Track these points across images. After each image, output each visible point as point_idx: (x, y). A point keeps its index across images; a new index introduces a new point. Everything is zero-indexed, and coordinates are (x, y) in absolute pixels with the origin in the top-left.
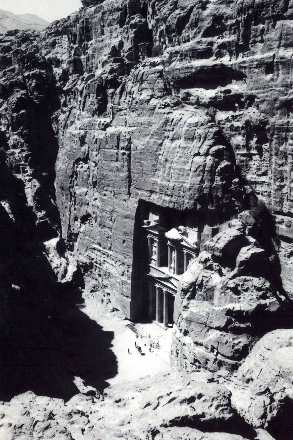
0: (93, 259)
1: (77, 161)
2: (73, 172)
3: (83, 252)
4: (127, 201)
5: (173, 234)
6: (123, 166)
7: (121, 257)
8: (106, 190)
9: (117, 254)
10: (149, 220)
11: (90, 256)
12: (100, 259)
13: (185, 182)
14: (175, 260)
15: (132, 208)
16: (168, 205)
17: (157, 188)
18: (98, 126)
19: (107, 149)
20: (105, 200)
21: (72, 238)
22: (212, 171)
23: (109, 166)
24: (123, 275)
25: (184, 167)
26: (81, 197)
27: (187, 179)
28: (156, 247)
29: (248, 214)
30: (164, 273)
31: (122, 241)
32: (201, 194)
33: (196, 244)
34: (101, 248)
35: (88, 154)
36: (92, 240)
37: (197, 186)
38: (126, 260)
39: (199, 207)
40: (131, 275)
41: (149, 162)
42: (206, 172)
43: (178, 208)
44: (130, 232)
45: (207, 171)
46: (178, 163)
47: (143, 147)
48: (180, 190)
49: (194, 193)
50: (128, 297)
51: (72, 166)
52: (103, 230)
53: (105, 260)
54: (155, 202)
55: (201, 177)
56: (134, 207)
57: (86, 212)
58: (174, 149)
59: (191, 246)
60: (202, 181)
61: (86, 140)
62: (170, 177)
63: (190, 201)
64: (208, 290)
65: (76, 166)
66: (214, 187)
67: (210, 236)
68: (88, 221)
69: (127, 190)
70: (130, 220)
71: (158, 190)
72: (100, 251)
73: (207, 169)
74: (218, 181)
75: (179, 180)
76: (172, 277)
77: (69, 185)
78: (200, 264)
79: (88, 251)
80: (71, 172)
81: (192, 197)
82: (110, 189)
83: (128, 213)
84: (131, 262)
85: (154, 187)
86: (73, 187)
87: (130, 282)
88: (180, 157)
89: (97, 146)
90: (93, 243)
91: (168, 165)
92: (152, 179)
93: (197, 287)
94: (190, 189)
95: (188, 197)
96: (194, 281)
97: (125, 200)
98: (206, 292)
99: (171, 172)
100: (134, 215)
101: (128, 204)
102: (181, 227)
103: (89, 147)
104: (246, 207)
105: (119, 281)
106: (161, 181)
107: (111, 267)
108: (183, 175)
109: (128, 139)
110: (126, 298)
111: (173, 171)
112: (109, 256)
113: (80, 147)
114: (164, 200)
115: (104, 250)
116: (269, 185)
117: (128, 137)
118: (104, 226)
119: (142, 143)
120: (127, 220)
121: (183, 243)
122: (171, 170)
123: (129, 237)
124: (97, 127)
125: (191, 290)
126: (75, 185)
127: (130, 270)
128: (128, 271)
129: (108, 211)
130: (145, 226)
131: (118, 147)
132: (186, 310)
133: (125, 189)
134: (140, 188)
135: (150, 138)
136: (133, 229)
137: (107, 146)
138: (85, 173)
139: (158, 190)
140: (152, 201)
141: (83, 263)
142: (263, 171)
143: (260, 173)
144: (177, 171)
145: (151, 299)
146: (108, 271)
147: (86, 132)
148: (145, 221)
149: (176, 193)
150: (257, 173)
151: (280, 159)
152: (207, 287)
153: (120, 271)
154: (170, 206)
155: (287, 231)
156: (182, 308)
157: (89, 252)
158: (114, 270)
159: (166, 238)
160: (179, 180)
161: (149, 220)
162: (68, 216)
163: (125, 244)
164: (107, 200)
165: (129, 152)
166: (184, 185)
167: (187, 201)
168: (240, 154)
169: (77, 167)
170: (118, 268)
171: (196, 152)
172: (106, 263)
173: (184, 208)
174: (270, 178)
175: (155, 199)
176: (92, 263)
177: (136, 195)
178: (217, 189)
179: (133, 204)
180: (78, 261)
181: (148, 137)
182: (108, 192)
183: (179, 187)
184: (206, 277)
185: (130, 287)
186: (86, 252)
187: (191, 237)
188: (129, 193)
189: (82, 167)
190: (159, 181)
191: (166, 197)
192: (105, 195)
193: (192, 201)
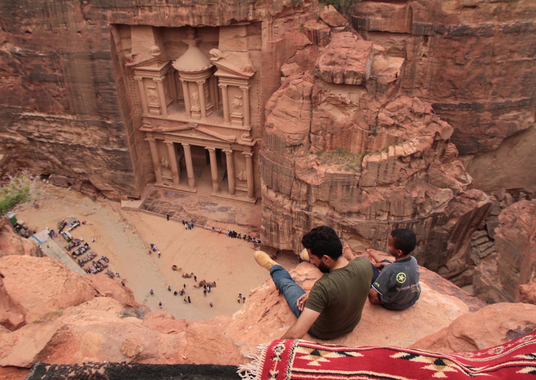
0: (31, 134)
20: (30, 40)
24: (106, 144)
29: (335, 10)
31: (94, 95)
33: (250, 70)
34: (42, 115)
53: (59, 129)
56: (104, 39)
59: (242, 75)
70: (102, 60)
72: (43, 119)
90: (24, 110)
93: (312, 136)
101: (89, 37)
105: (100, 152)
107: (75, 137)
112: (62, 124)
114: (177, 16)
115: (51, 116)
123: (107, 87)
125: (305, 141)
128: (117, 137)
130: (128, 64)
146: (70, 144)
153: (98, 138)
154: (191, 24)
155: (385, 24)
161: (133, 53)
167: (230, 9)
172: (62, 134)
182: (34, 26)
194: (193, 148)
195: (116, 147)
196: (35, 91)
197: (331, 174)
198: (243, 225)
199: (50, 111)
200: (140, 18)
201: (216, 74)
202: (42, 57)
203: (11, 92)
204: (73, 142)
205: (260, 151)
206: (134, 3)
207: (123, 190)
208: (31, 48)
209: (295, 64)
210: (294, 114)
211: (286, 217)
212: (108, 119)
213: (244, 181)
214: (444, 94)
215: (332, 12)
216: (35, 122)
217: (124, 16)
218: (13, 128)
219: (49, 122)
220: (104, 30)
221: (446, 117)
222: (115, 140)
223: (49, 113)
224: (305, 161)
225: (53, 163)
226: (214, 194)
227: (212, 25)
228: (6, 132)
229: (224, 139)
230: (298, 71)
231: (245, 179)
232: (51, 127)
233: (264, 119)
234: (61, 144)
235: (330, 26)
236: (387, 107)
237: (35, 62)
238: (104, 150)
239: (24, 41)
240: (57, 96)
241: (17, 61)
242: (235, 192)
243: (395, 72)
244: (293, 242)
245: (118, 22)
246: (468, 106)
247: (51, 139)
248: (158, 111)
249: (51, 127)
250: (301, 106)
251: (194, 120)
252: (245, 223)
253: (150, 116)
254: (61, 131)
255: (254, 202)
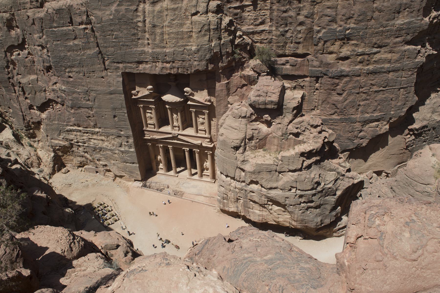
0: (72, 140)
1: (11, 49)
2: (8, 61)
3: (55, 136)
4: (106, 78)
5: (168, 98)
6: (89, 43)
7: (114, 131)
8: (69, 72)
9: (108, 129)
10: (137, 90)
11: (68, 138)
12: (82, 138)
13: (188, 45)
14: (177, 120)
15: (115, 83)
16: (169, 71)
17: (148, 57)
18: (29, 4)
19: (55, 27)
20: (71, 82)
21: (31, 127)
22: (218, 28)
23: (66, 46)
24: (120, 146)
25: (181, 30)
26: (31, 85)
27: (190, 42)
28: (151, 113)
29: (261, 63)
30: (170, 134)
32: (212, 53)
34: (80, 128)
35: (24, 40)
36: (65, 124)
37: (207, 46)
38: (122, 133)
39: (211, 67)
40: (133, 144)
41: (125, 32)
42: (212, 30)
43: (184, 72)
44: (120, 106)
45: (213, 29)
46: (172, 27)
47: (111, 17)
48: (183, 54)
49: (205, 54)
50: (133, 163)
51: (4, 55)
52: (79, 111)
53: (90, 137)
54: (147, 72)
55: (208, 36)
57: (46, 99)
58: (160, 12)
60: (210, 41)
61: (14, 24)
62: (165, 43)
63: (201, 63)
64: (260, 140)
65: (9, 54)
66: (223, 44)
67: (224, 91)
68: (51, 107)
69: (103, 66)
70: (117, 95)
71: (149, 58)
72: (80, 131)
73: (212, 27)
74: (226, 38)
75: (179, 44)
76: (179, 134)
77: (7, 76)
78: (240, 119)
79: (62, 134)
80: (5, 62)
81: (202, 58)
82: (74, 69)
83: (112, 89)
84: (131, 133)
85: (142, 56)
86: (13, 77)
87: (133, 150)
88: (173, 20)
89: (37, 27)
90: (67, 125)
91: (158, 31)
92: (135, 49)
93: (247, 140)
94: (198, 50)
95: (197, 59)
96: (244, 136)
97: (103, 77)
98: (259, 142)
99: (165, 38)
100: (122, 89)
101: (109, 80)
102: (186, 89)
103: (23, 30)
104: (252, 55)
106: (153, 49)
107: (101, 142)
108: (182, 39)
109: (84, 12)
110: (131, 165)
111: (167, 37)
112: (93, 134)
113: (8, 33)
114: (163, 68)
115: (85, 129)
116: (270, 32)
117: (84, 9)
118: (79, 108)
119: (108, 13)
120: (112, 96)
121: (189, 103)
122: (165, 36)
123: (121, 111)
124: (28, 6)
125: (243, 144)
126: (16, 74)
127: (131, 140)
128: (127, 142)
129: (81, 92)
130: (134, 97)
131: (71, 22)
132: (245, 163)
133: (99, 66)
134: (120, 61)
135: (118, 5)
136: (124, 102)
137: (55, 25)
138: (27, 60)
139: (149, 58)
140: (142, 72)
141: (60, 146)
142: (260, 20)
143: (258, 22)
144: (173, 35)
145: (153, 157)
146: (97, 147)
147: (13, 15)
148: (133, 92)
149: (179, 57)
150: (254, 23)
151: (283, 5)
152: (260, 138)
154: (173, 73)
155: (292, 70)
156: (239, 163)
157: (64, 135)
158: (106, 143)
159: (164, 101)
160: (179, 44)
162: (18, 107)
163: (116, 119)
164: (75, 82)
165: (91, 26)
166: (188, 48)
168: (232, 8)
169: (12, 55)
170: (113, 142)
171: (194, 11)
172: (92, 140)
173: (193, 71)
174: (270, 26)
175: (144, 68)
176: (72, 144)
177: (116, 69)
178: (226, 45)
179: (115, 80)
180: (52, 146)
181: (115, 5)
183: (182, 51)
184: (256, 129)
185: (135, 154)
186: (60, 135)
187: (201, 97)
188: (106, 69)
189: (19, 54)
190: (146, 49)
191: (165, 64)
192: (70, 77)
193: (204, 63)
194: (174, 149)
195: (127, 149)
196: (74, 114)
197: (259, 164)
198: (207, 197)
199: (85, 126)
200: (140, 68)
201: (189, 103)
202: (79, 92)
203: (60, 115)
204: (99, 145)
205: (216, 150)
206: (137, 59)
207: (131, 175)
208: (72, 87)
209: (236, 96)
210: (236, 128)
211: (233, 192)
212: (122, 131)
213: (207, 169)
214: (330, 113)
215: (258, 63)
216: (75, 133)
217: (131, 68)
218: (60, 136)
219: (84, 133)
220: (118, 76)
221: (332, 127)
222: (126, 144)
223: (84, 128)
224: (243, 156)
225: (87, 159)
226: (188, 177)
227: (185, 73)
228: (57, 139)
229: (194, 143)
230: (238, 101)
231: (208, 167)
232: (85, 136)
233: (218, 131)
234: (92, 147)
235: (257, 73)
236: (293, 122)
237: (75, 95)
238: (119, 150)
239: (68, 82)
240: (89, 117)
241: (64, 95)
242: (201, 176)
243: (298, 100)
244: (237, 207)
245: (127, 71)
246: (346, 119)
247: (85, 143)
248: (153, 126)
249: (85, 136)
250: (240, 122)
251: (176, 132)
252: (208, 195)
253: (148, 129)
254: (92, 139)
255: (214, 181)
